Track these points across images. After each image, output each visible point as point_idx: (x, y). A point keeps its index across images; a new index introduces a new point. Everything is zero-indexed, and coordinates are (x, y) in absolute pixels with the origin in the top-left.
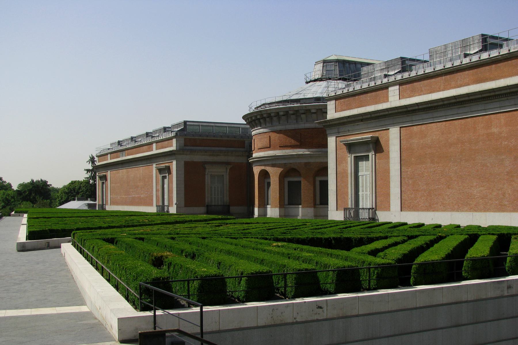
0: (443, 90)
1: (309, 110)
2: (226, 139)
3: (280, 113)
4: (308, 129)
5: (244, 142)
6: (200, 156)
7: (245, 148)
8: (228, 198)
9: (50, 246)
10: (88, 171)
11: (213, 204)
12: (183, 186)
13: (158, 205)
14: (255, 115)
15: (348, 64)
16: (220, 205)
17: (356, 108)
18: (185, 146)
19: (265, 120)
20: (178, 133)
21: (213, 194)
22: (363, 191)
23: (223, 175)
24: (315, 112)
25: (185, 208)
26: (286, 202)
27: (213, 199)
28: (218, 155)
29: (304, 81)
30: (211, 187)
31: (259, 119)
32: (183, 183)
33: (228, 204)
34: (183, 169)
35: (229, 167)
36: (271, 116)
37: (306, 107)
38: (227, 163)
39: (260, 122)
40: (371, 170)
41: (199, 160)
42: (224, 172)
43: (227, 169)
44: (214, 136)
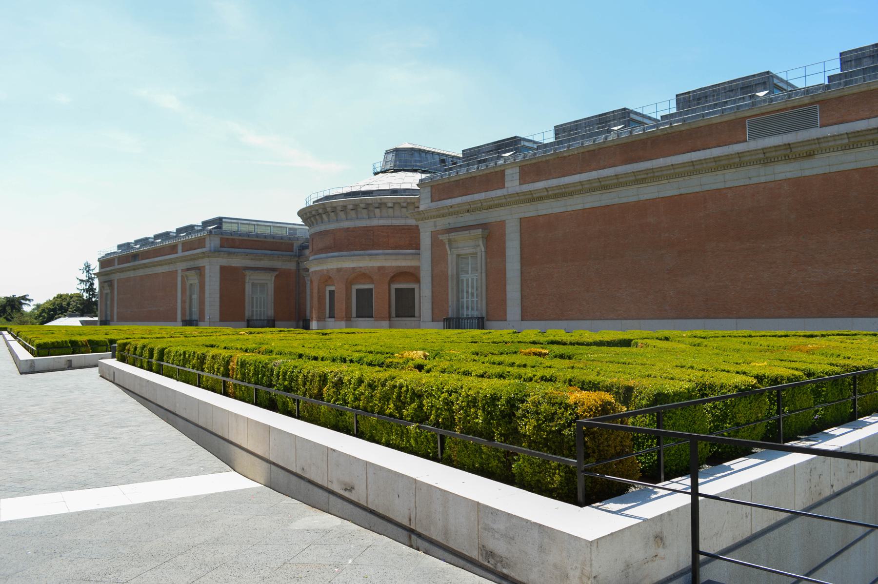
0: (580, 173)
1: (385, 204)
2: (272, 240)
3: (348, 206)
4: (384, 226)
5: (292, 245)
7: (293, 251)
8: (273, 311)
9: (73, 366)
10: (82, 281)
11: (255, 318)
12: (218, 296)
13: (184, 319)
14: (317, 208)
15: (424, 154)
16: (264, 320)
17: (460, 196)
18: (221, 247)
19: (328, 216)
20: (213, 231)
22: (467, 297)
23: (267, 284)
24: (392, 206)
25: (221, 322)
26: (354, 314)
27: (255, 312)
28: (261, 260)
29: (372, 172)
30: (253, 298)
32: (218, 291)
33: (272, 318)
34: (218, 275)
35: (276, 273)
36: (328, 212)
37: (381, 200)
38: (272, 270)
39: (316, 220)
40: (479, 271)
41: (238, 265)
42: (269, 280)
43: (272, 276)
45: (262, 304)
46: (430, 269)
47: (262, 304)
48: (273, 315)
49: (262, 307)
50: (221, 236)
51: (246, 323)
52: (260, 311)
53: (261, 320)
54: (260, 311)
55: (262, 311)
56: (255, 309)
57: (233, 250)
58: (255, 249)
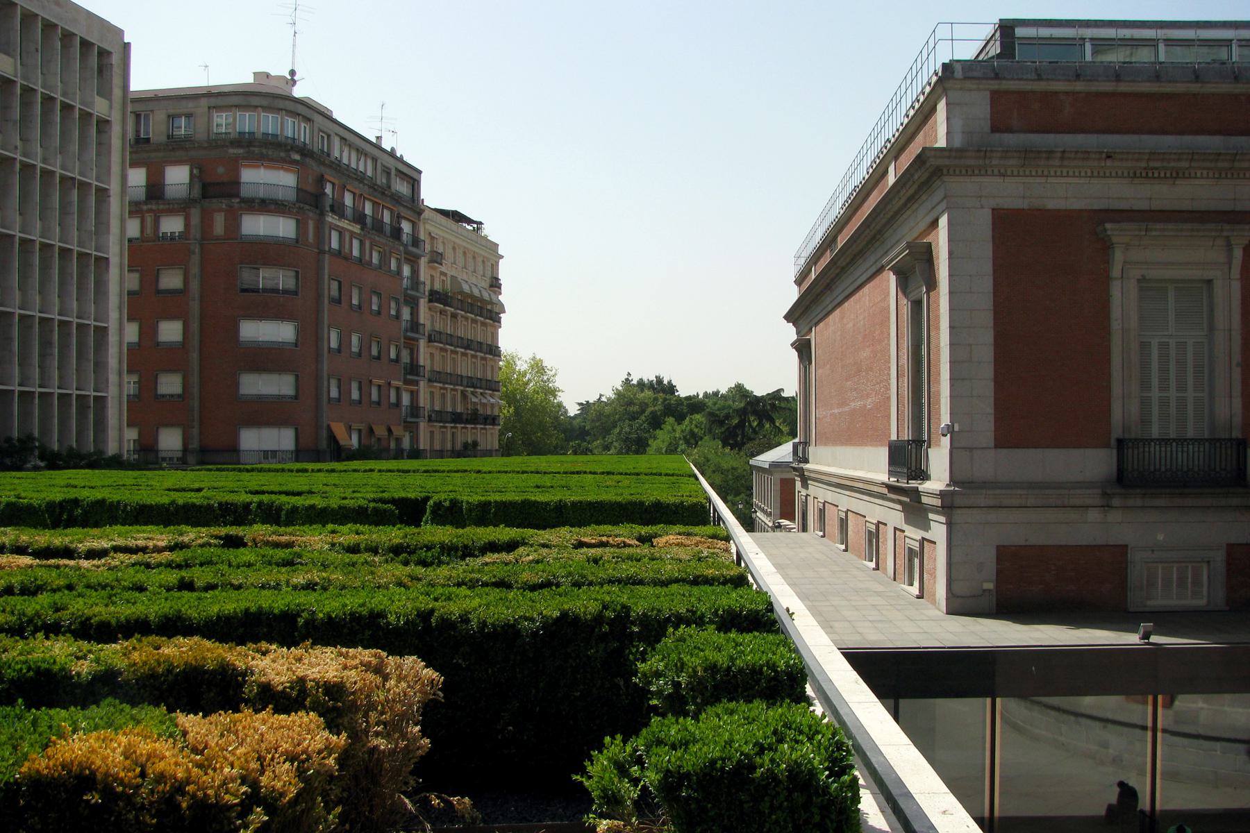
2: (1226, 88)
6: (1082, 181)
8: (1237, 404)
12: (988, 337)
16: (1194, 440)
18: (995, 129)
21: (1155, 382)
23: (1209, 282)
25: (999, 450)
30: (1144, 346)
32: (987, 318)
33: (1236, 434)
34: (987, 250)
41: (1075, 204)
43: (1229, 247)
44: (1157, 77)
45: (1190, 370)
47: (1190, 370)
48: (1238, 420)
49: (1173, 384)
50: (995, 85)
51: (1115, 452)
53: (1181, 441)
55: (1173, 404)
56: (1155, 394)
57: (1050, 139)
58: (1152, 132)
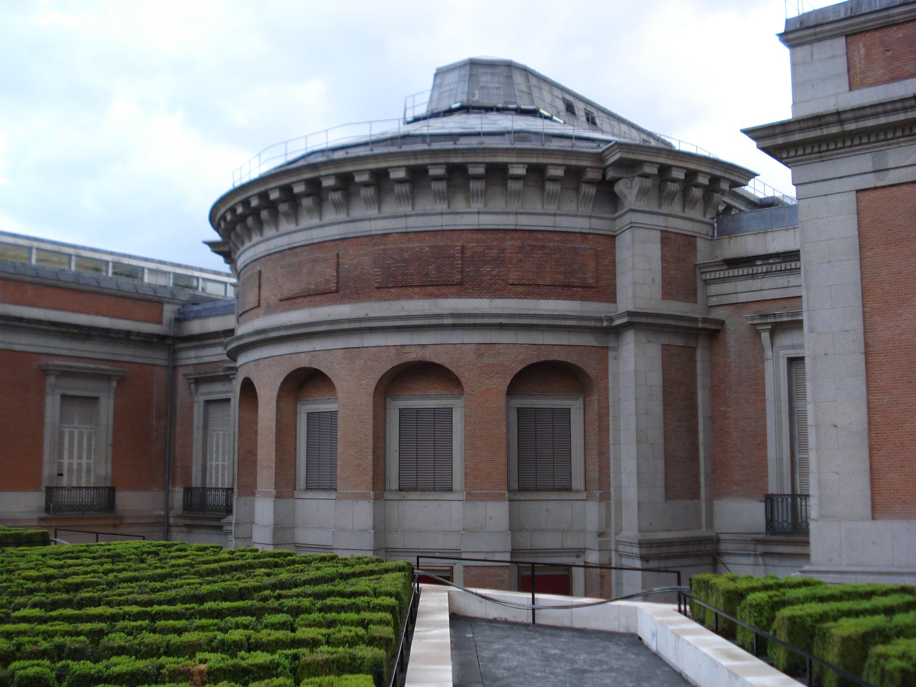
16: (86, 488)
31: (256, 212)
33: (109, 484)
46: (857, 324)
48: (110, 475)
52: (80, 465)
53: (80, 488)
54: (80, 465)
56: (66, 461)
